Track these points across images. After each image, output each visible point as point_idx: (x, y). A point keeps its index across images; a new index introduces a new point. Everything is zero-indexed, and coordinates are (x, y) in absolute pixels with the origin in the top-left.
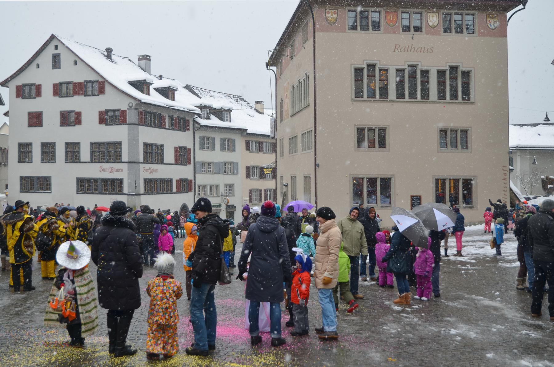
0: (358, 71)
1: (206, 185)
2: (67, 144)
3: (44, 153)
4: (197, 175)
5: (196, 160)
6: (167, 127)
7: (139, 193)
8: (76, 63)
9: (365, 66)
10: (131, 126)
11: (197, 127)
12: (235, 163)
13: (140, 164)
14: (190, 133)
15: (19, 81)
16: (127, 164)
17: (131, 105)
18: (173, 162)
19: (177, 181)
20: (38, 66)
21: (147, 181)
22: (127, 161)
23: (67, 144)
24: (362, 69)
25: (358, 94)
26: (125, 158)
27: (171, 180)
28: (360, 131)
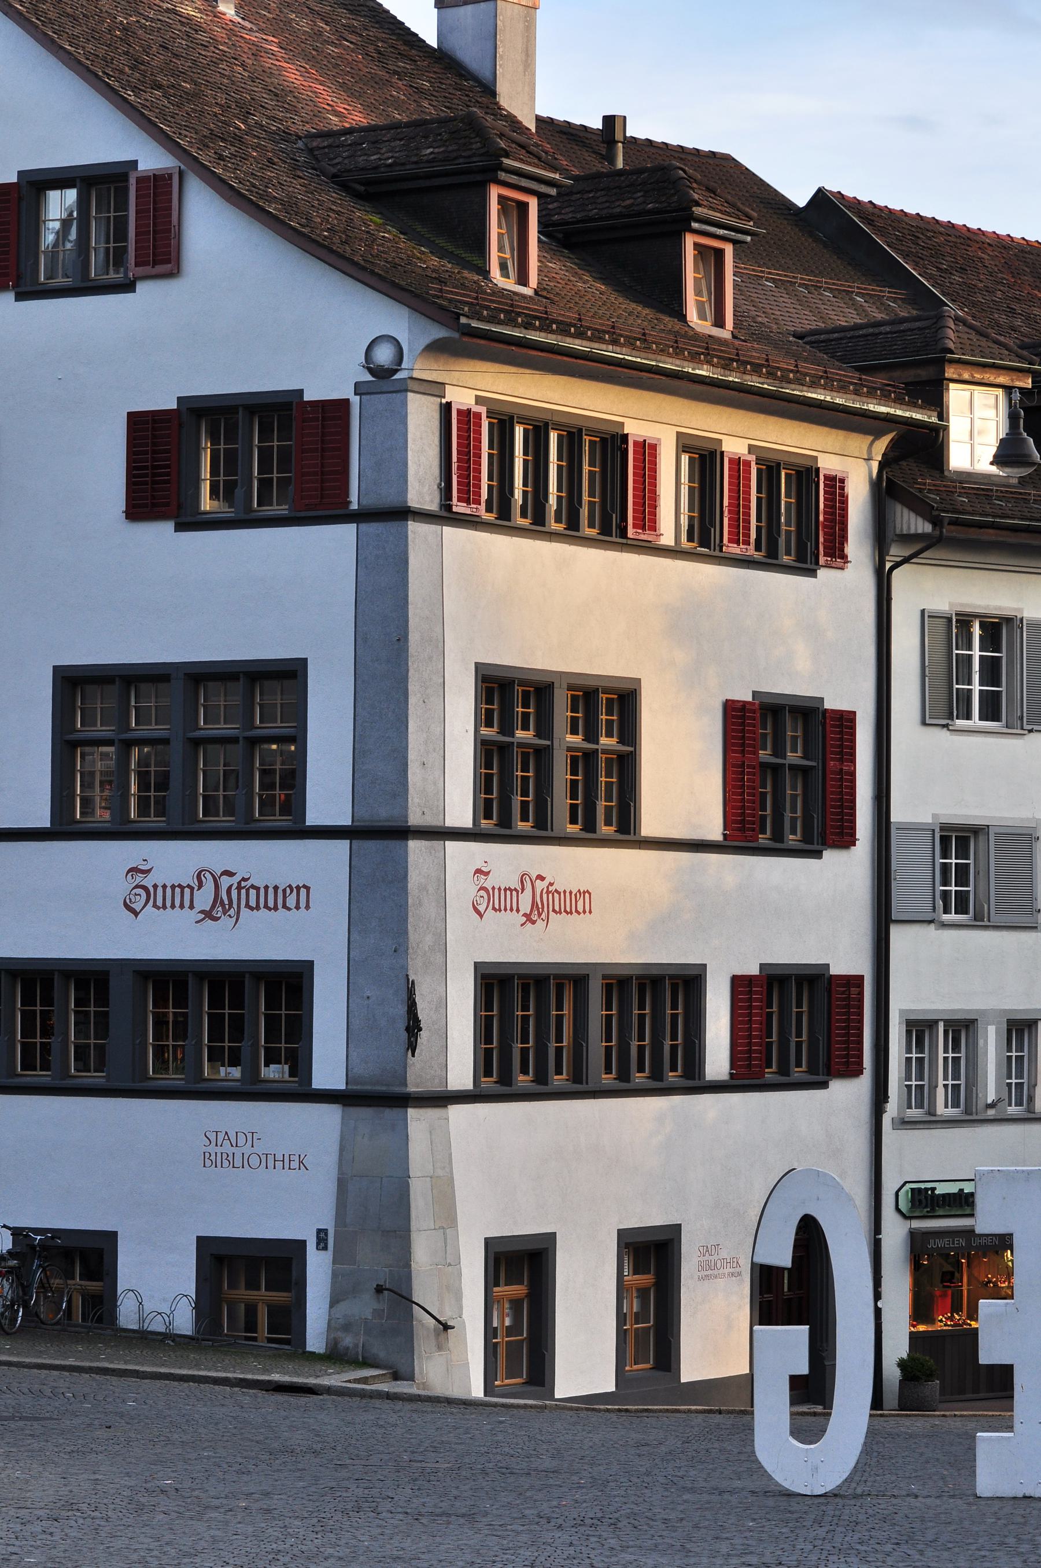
4: (900, 938)
5: (898, 815)
6: (667, 534)
10: (371, 528)
11: (907, 539)
13: (451, 846)
16: (342, 846)
17: (384, 355)
18: (714, 831)
19: (740, 985)
22: (345, 820)
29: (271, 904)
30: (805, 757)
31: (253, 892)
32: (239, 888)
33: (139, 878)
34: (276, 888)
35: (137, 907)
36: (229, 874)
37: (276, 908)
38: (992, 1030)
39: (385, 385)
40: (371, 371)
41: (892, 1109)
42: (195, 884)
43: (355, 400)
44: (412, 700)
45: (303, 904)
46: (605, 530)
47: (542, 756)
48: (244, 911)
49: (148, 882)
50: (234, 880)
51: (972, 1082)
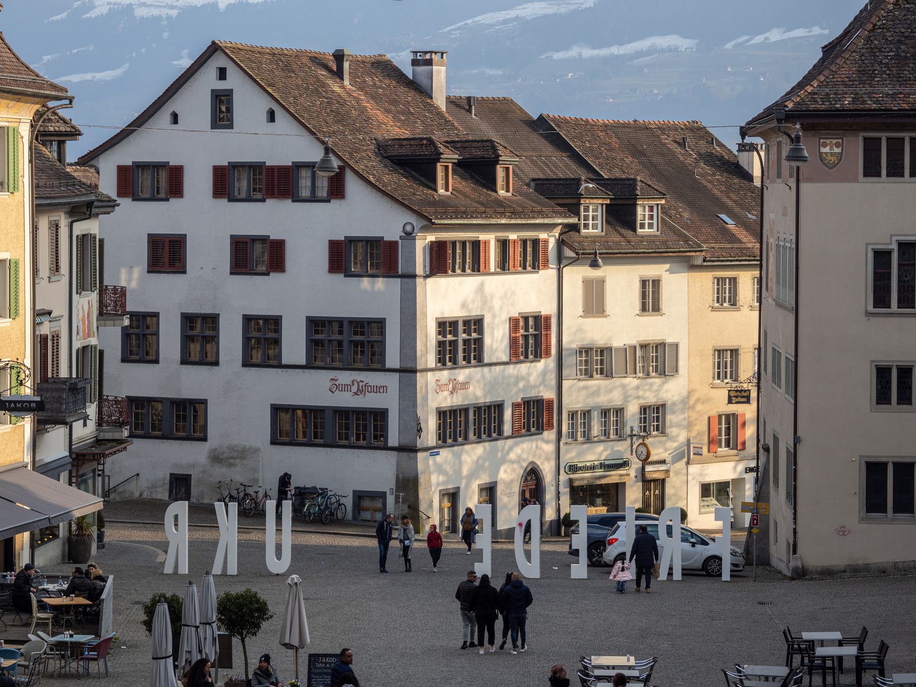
0: (881, 257)
1: (589, 412)
2: (248, 320)
3: (187, 339)
4: (566, 384)
6: (492, 270)
7: (425, 446)
8: (272, 117)
9: (895, 246)
10: (405, 280)
12: (671, 345)
13: (430, 374)
14: (548, 275)
15: (127, 154)
16: (397, 375)
17: (409, 228)
20: (175, 118)
21: (442, 414)
23: (248, 320)
24: (889, 253)
25: (881, 299)
26: (393, 358)
27: (499, 407)
28: (883, 373)
29: (375, 391)
30: (535, 330)
31: (369, 387)
32: (365, 386)
33: (334, 382)
34: (377, 386)
35: (333, 390)
36: (362, 382)
37: (377, 392)
38: (596, 413)
39: (409, 237)
40: (405, 233)
41: (563, 441)
42: (352, 384)
43: (400, 241)
44: (418, 332)
45: (385, 391)
46: (473, 270)
47: (454, 343)
48: (367, 393)
49: (337, 383)
50: (364, 383)
51: (590, 430)
